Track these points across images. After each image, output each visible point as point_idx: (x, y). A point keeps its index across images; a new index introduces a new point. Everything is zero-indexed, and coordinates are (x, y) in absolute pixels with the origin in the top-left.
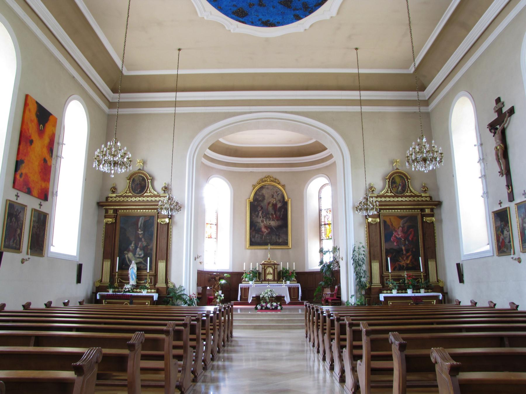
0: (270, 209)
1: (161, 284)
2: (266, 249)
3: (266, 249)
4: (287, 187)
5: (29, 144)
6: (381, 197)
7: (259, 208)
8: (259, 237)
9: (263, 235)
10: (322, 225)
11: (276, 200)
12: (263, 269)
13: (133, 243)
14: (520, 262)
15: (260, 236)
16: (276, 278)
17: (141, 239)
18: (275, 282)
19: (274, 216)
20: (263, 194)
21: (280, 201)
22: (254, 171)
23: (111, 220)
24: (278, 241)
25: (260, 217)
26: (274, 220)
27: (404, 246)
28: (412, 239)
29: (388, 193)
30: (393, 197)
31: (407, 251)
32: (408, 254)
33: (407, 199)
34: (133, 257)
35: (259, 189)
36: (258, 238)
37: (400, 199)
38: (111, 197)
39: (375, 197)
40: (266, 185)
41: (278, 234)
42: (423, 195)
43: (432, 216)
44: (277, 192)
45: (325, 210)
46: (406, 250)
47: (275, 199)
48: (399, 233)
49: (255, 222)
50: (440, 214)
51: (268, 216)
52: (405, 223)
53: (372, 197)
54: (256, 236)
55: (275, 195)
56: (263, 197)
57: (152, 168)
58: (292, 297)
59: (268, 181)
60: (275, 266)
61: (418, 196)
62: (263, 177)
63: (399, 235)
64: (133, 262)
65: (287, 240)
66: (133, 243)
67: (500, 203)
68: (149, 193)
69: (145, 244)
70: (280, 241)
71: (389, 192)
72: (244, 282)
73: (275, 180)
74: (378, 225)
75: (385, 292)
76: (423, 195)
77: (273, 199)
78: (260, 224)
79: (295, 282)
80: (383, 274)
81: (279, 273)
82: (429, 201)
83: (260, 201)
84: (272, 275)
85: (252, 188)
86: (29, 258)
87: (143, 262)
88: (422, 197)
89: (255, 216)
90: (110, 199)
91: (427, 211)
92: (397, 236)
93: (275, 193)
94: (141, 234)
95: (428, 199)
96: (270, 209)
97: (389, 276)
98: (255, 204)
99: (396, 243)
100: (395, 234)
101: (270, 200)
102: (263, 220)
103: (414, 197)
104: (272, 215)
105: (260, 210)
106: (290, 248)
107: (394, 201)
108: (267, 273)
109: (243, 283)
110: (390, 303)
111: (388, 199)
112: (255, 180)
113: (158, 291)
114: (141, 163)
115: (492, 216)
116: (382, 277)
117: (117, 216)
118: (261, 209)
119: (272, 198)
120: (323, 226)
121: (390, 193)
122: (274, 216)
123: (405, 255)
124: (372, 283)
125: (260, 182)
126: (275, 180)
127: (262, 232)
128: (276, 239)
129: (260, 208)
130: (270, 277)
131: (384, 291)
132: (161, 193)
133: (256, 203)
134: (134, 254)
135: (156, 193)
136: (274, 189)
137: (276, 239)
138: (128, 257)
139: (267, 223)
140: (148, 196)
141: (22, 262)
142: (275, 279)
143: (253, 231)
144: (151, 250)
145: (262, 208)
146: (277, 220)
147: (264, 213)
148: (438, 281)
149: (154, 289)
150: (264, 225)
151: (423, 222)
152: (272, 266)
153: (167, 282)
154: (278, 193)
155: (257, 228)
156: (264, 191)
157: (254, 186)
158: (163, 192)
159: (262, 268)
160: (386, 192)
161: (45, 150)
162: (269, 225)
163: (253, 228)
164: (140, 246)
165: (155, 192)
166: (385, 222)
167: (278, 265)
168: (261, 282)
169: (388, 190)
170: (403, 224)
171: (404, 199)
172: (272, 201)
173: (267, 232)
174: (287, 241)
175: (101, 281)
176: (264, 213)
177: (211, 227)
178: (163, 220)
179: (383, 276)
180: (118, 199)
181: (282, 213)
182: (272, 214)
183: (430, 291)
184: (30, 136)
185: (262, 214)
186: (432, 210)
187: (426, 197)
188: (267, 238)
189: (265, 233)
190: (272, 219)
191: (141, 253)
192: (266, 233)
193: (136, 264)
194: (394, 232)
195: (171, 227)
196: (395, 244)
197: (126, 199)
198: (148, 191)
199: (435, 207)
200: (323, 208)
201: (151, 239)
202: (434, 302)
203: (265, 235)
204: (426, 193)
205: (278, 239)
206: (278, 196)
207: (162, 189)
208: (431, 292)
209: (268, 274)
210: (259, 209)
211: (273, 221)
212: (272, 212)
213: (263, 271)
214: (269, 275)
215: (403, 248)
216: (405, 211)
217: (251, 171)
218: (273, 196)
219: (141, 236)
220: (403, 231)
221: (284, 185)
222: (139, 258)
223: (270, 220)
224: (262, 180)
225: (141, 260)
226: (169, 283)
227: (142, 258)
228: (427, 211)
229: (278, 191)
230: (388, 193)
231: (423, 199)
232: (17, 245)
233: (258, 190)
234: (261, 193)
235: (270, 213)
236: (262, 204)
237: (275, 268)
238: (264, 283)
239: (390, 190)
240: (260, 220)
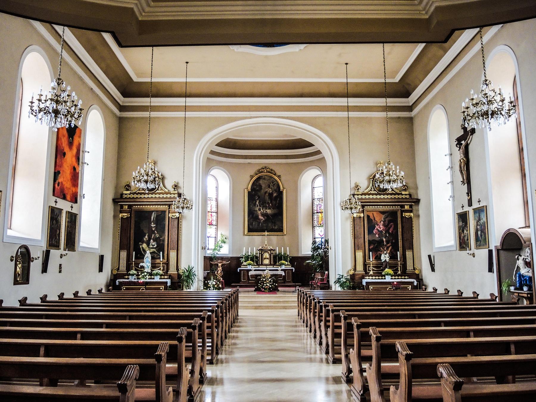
1: (172, 271)
2: (263, 235)
3: (263, 235)
4: (283, 178)
5: (63, 156)
6: (365, 194)
9: (260, 222)
10: (314, 213)
11: (272, 190)
13: (147, 235)
14: (474, 257)
15: (257, 223)
17: (154, 231)
18: (271, 266)
19: (270, 204)
21: (275, 190)
22: (252, 162)
23: (126, 215)
24: (274, 227)
25: (258, 206)
27: (385, 238)
28: (392, 232)
29: (372, 191)
30: (376, 195)
31: (388, 242)
32: (388, 245)
33: (389, 197)
34: (147, 248)
37: (382, 196)
38: (126, 194)
39: (360, 194)
41: (273, 221)
42: (403, 193)
43: (411, 211)
44: (273, 182)
46: (386, 241)
48: (381, 226)
50: (418, 210)
51: (264, 204)
52: (386, 218)
53: (358, 195)
56: (260, 186)
57: (164, 168)
59: (264, 172)
61: (398, 194)
63: (380, 228)
64: (148, 252)
66: (147, 235)
67: (463, 207)
68: (161, 190)
69: (157, 236)
70: (276, 228)
71: (373, 190)
72: (243, 267)
73: (272, 171)
74: (362, 218)
75: (367, 277)
76: (403, 193)
77: (269, 189)
79: (289, 266)
80: (366, 262)
81: (275, 257)
82: (409, 199)
83: (257, 190)
85: (249, 179)
86: (67, 254)
87: (156, 252)
88: (402, 195)
90: (125, 196)
91: (407, 207)
92: (379, 229)
94: (154, 227)
95: (408, 197)
96: (267, 198)
97: (370, 264)
98: (253, 194)
99: (378, 235)
100: (377, 227)
103: (395, 194)
105: (257, 199)
107: (377, 199)
109: (242, 267)
110: (371, 287)
111: (371, 196)
112: (252, 171)
113: (170, 277)
114: (152, 163)
115: (457, 216)
116: (365, 265)
117: (131, 211)
120: (315, 214)
121: (374, 191)
122: (270, 204)
123: (386, 245)
124: (356, 270)
127: (259, 219)
128: (272, 226)
130: (267, 262)
131: (366, 277)
132: (172, 190)
134: (148, 245)
135: (167, 190)
137: (272, 226)
138: (142, 247)
139: (264, 211)
140: (160, 194)
141: (61, 257)
144: (164, 241)
148: (414, 269)
149: (167, 276)
151: (402, 217)
153: (178, 269)
154: (274, 183)
155: (254, 216)
156: (261, 182)
157: (252, 177)
158: (173, 189)
160: (370, 191)
161: (74, 159)
164: (153, 237)
165: (165, 189)
166: (368, 216)
168: (258, 267)
169: (372, 189)
170: (384, 219)
171: (386, 197)
174: (282, 228)
175: (118, 269)
177: (211, 215)
178: (174, 214)
179: (366, 264)
180: (132, 196)
181: (278, 202)
183: (406, 277)
184: (63, 150)
185: (259, 203)
186: (411, 206)
187: (406, 195)
191: (154, 244)
193: (151, 253)
194: (376, 226)
195: (181, 221)
196: (377, 236)
197: (139, 196)
198: (160, 189)
199: (414, 204)
200: (316, 197)
201: (163, 232)
202: (409, 287)
204: (406, 191)
207: (172, 187)
208: (407, 278)
209: (265, 258)
210: (257, 198)
215: (384, 239)
216: (386, 207)
218: (269, 187)
219: (154, 229)
220: (384, 225)
221: (280, 176)
222: (152, 248)
223: (266, 209)
224: (259, 171)
225: (155, 250)
226: (180, 270)
227: (155, 248)
228: (407, 207)
230: (372, 191)
231: (403, 196)
232: (57, 243)
236: (259, 194)
237: (271, 253)
239: (374, 189)
240: (257, 209)
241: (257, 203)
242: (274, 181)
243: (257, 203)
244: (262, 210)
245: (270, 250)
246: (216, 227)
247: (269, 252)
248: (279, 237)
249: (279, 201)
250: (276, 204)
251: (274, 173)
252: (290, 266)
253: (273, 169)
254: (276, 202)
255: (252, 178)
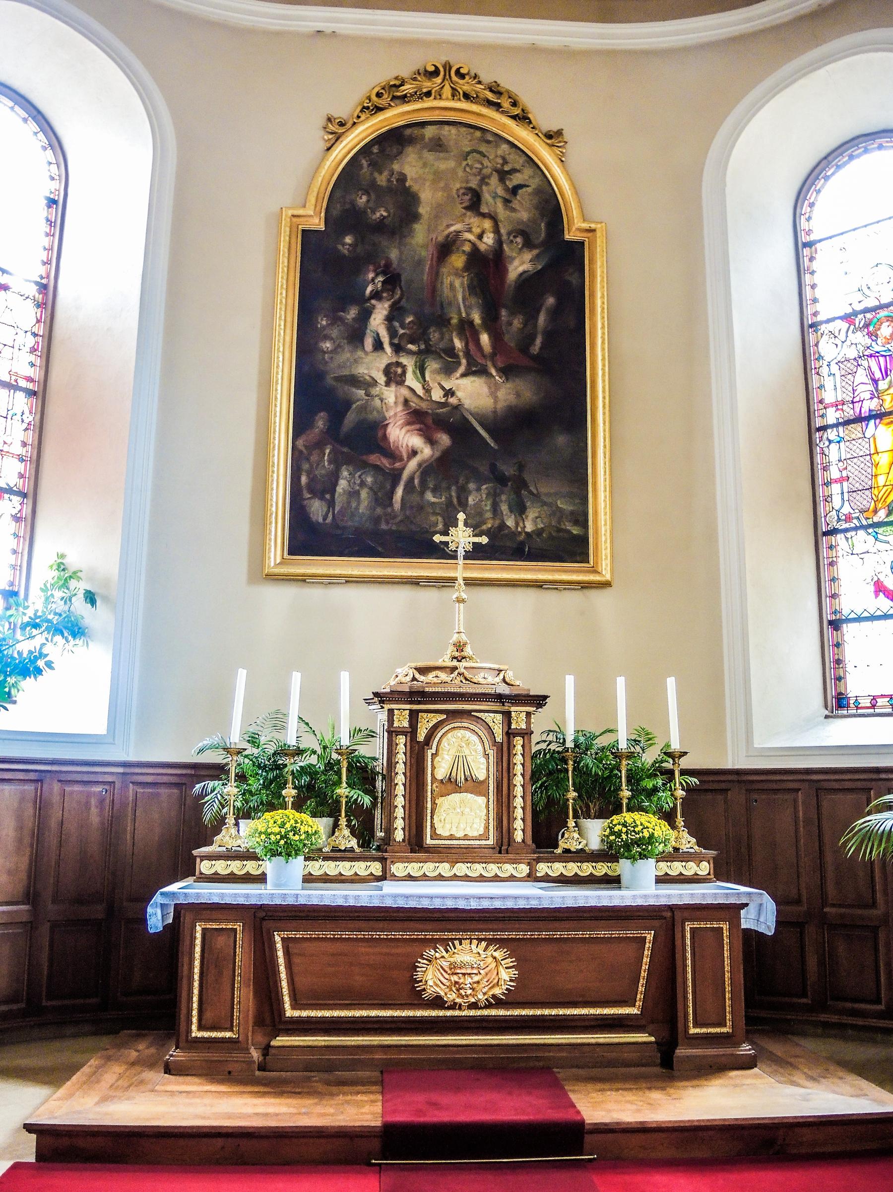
0: (452, 285)
7: (371, 275)
8: (364, 494)
9: (395, 477)
10: (823, 428)
11: (496, 230)
12: (401, 740)
16: (518, 824)
18: (508, 869)
19: (485, 338)
20: (402, 179)
21: (523, 233)
24: (510, 522)
26: (482, 372)
35: (375, 149)
36: (357, 493)
40: (423, 124)
41: (508, 469)
44: (503, 175)
45: (848, 318)
47: (493, 218)
49: (338, 379)
54: (342, 485)
55: (495, 196)
58: (693, 1031)
60: (507, 715)
62: (405, 73)
65: (581, 518)
70: (529, 528)
78: (375, 391)
79: (690, 869)
83: (380, 227)
84: (482, 800)
85: (319, 140)
89: (335, 332)
93: (494, 180)
98: (345, 250)
101: (457, 227)
102: (398, 364)
104: (467, 328)
105: (376, 295)
106: (606, 585)
108: (441, 774)
109: (205, 867)
118: (383, 282)
119: (469, 213)
120: (832, 434)
122: (485, 338)
125: (382, 102)
126: (490, 96)
127: (392, 454)
129: (380, 279)
133: (348, 240)
136: (480, 153)
139: (428, 391)
142: (510, 831)
143: (319, 445)
145: (392, 280)
146: (507, 372)
147: (409, 319)
150: (406, 402)
152: (488, 717)
154: (516, 179)
155: (351, 418)
159: (392, 733)
162: (444, 405)
163: (321, 422)
167: (539, 701)
168: (376, 868)
172: (470, 230)
173: (427, 452)
174: (575, 531)
176: (409, 319)
181: (542, 319)
182: (471, 323)
185: (389, 319)
188: (430, 497)
189: (413, 464)
190: (464, 361)
192: (420, 465)
203: (411, 479)
205: (511, 511)
206: (515, 204)
209: (451, 785)
210: (373, 281)
211: (474, 373)
212: (468, 308)
213: (401, 757)
214: (455, 797)
217: (320, 26)
218: (474, 203)
221: (560, 133)
223: (448, 370)
229: (514, 171)
233: (365, 151)
234: (386, 173)
235: (454, 321)
236: (394, 254)
237: (510, 734)
238: (410, 878)
241: (378, 321)
242: (516, 161)
243: (378, 321)
244: (411, 380)
245: (499, 698)
246: (27, 510)
247: (496, 721)
248: (549, 597)
249: (555, 313)
250: (527, 339)
251: (516, 111)
252: (704, 868)
253: (505, 83)
254: (531, 317)
255: (338, 138)
